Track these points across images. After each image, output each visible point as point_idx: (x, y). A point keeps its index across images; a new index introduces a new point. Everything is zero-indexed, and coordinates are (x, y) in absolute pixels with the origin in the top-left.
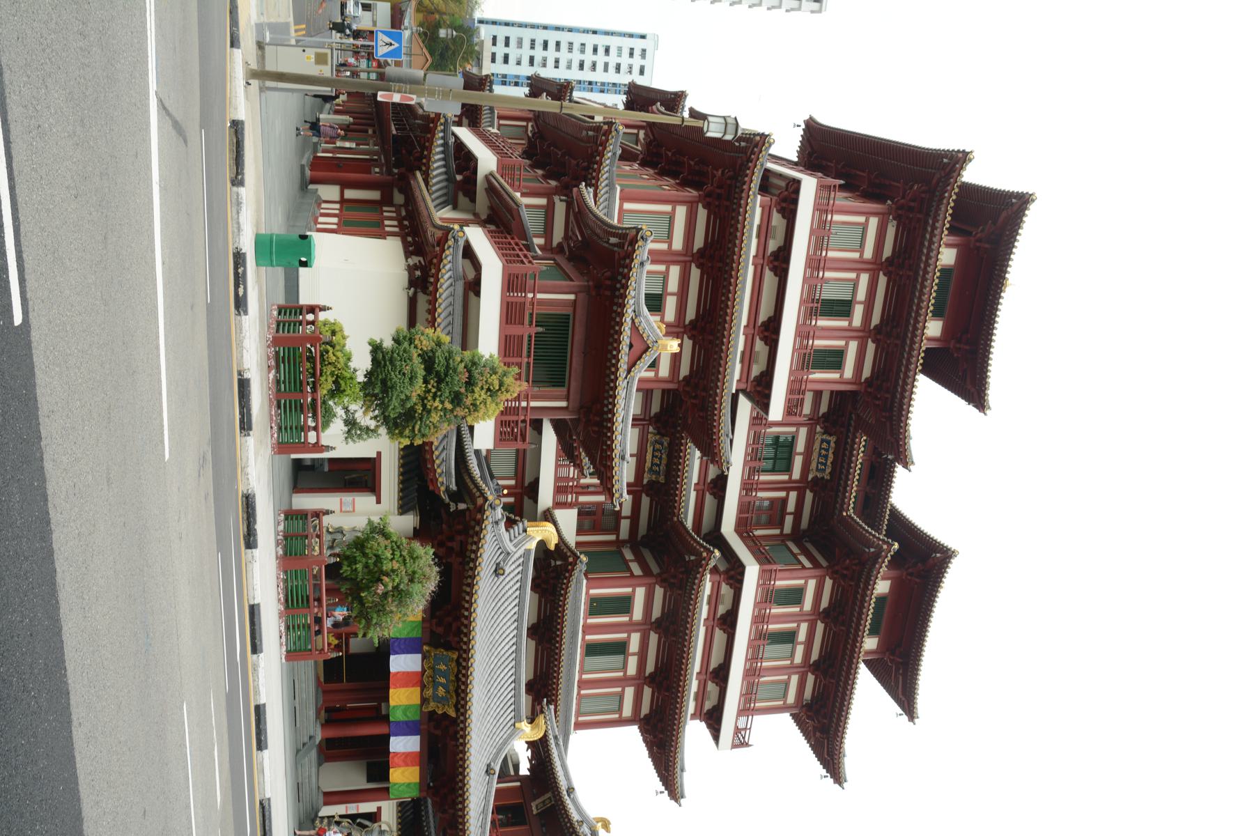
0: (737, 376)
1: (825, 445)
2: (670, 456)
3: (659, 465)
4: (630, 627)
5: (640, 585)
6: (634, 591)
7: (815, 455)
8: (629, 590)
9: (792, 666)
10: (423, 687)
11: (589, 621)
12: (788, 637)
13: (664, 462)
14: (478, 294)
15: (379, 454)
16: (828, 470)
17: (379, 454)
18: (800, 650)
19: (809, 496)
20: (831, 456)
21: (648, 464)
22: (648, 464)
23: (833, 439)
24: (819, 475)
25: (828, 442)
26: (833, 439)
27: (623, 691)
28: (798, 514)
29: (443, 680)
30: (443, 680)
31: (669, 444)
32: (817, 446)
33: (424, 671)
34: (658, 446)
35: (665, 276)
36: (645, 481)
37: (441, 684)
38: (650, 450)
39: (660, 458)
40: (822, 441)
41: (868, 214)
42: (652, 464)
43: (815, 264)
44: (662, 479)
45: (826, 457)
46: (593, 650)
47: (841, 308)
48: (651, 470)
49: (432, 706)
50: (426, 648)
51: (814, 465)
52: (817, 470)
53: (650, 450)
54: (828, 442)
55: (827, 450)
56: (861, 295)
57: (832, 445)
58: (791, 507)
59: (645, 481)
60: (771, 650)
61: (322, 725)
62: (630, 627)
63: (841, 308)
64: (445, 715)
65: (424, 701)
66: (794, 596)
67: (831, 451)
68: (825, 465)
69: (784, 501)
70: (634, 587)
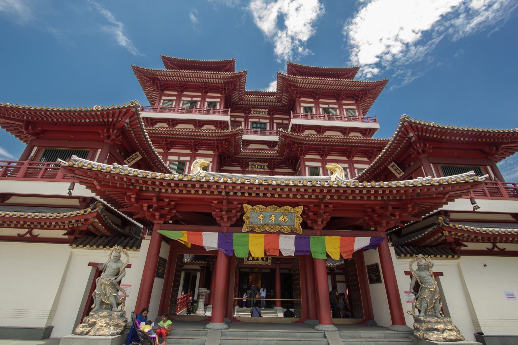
3: (261, 166)
5: (304, 164)
6: (307, 166)
7: (259, 115)
8: (307, 168)
9: (339, 108)
10: (279, 233)
12: (326, 110)
13: (259, 164)
15: (90, 264)
16: (264, 110)
17: (90, 264)
18: (331, 106)
20: (259, 110)
21: (261, 170)
22: (261, 170)
23: (252, 110)
24: (267, 113)
25: (254, 111)
26: (252, 110)
27: (356, 168)
28: (283, 119)
30: (273, 217)
31: (252, 162)
33: (265, 232)
34: (253, 167)
37: (277, 218)
40: (254, 113)
41: (160, 99)
42: (261, 168)
45: (259, 111)
47: (193, 104)
54: (254, 111)
55: (257, 111)
56: (190, 99)
57: (255, 110)
58: (280, 121)
61: (320, 323)
63: (193, 104)
66: (308, 110)
68: (262, 112)
69: (277, 124)
70: (305, 166)
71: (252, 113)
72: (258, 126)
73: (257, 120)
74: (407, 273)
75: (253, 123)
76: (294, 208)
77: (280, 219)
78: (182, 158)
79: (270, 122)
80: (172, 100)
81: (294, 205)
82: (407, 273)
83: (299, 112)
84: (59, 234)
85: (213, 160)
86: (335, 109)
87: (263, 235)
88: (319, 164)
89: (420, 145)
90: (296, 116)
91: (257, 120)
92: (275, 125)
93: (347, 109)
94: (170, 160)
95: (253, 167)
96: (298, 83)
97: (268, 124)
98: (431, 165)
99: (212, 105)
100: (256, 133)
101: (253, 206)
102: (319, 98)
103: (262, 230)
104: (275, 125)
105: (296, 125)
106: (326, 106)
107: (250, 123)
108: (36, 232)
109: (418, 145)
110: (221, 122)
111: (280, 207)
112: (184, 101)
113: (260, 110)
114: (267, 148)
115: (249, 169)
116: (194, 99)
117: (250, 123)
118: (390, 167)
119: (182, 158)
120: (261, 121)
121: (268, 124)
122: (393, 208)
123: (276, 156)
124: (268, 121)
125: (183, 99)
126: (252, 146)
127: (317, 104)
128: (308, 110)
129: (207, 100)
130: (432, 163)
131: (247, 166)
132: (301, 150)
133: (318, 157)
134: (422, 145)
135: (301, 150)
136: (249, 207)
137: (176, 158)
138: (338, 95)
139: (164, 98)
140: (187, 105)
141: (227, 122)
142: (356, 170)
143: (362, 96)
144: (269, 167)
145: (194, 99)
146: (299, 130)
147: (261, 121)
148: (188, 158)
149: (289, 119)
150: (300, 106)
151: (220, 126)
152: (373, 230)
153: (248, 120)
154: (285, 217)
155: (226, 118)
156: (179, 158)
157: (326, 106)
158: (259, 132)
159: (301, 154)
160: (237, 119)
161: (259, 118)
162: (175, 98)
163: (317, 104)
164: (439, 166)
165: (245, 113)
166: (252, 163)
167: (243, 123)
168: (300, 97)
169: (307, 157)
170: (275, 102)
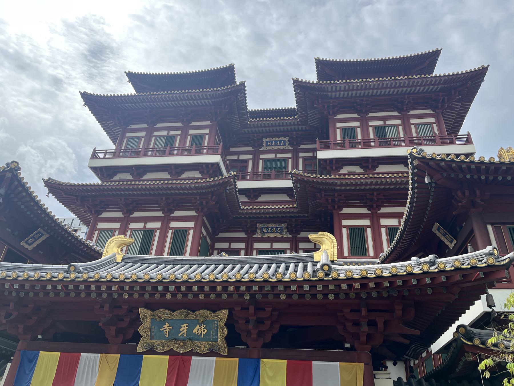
1: (269, 144)
2: (269, 222)
4: (376, 228)
5: (340, 223)
6: (345, 227)
7: (276, 148)
9: (404, 124)
11: (372, 254)
12: (380, 131)
13: (274, 225)
16: (283, 139)
18: (388, 122)
19: (302, 147)
20: (274, 139)
21: (277, 235)
22: (277, 235)
23: (264, 139)
24: (287, 143)
25: (267, 142)
26: (264, 139)
29: (184, 328)
30: (184, 328)
31: (261, 223)
34: (264, 231)
36: (291, 236)
38: (267, 235)
39: (272, 228)
40: (267, 145)
44: (284, 225)
45: (276, 142)
48: (280, 233)
49: (221, 342)
50: (140, 348)
51: (282, 147)
52: (285, 145)
53: (267, 235)
54: (267, 142)
55: (272, 142)
56: (165, 133)
59: (289, 236)
62: (376, 228)
63: (170, 140)
64: (227, 324)
65: (211, 353)
67: (273, 140)
68: (280, 141)
69: (305, 159)
71: (264, 144)
72: (274, 165)
73: (272, 156)
75: (266, 161)
76: (214, 312)
77: (195, 330)
78: (150, 225)
79: (292, 158)
80: (140, 138)
81: (214, 307)
83: (331, 138)
85: (196, 225)
86: (397, 126)
87: (167, 357)
88: (366, 222)
89: (464, 194)
90: (327, 147)
91: (272, 156)
92: (301, 161)
93: (416, 125)
94: (131, 229)
95: (264, 231)
96: (328, 91)
97: (290, 160)
98: (490, 228)
99: (198, 139)
100: (266, 177)
101: (153, 311)
102: (367, 112)
103: (166, 349)
104: (301, 161)
105: (325, 160)
106: (381, 123)
107: (261, 162)
109: (459, 193)
110: (207, 164)
111: (194, 311)
112: (157, 137)
113: (277, 139)
114: (287, 199)
115: (258, 235)
116: (172, 133)
117: (261, 162)
118: (435, 229)
119: (150, 225)
120: (279, 156)
121: (290, 160)
122: (369, 311)
123: (298, 212)
124: (289, 155)
125: (156, 133)
126: (263, 198)
127: (364, 122)
128: (349, 133)
129: (191, 132)
130: (492, 224)
131: (255, 232)
132: (333, 201)
133: (364, 210)
134: (467, 193)
135: (333, 201)
136: (148, 312)
137: (140, 225)
138: (402, 104)
139: (128, 135)
140: (161, 144)
141: (217, 164)
143: (444, 100)
144: (289, 231)
145: (172, 133)
146: (332, 168)
147: (279, 156)
148: (158, 225)
149: (314, 150)
150: (335, 128)
151: (208, 172)
152: (347, 349)
153: (259, 156)
154: (203, 327)
155: (216, 158)
156: (145, 225)
158: (273, 175)
159: (334, 207)
160: (242, 157)
162: (143, 134)
163: (364, 122)
164: (504, 229)
165: (253, 146)
166: (261, 225)
167: (250, 163)
168: (335, 114)
169: (345, 211)
170: (298, 125)
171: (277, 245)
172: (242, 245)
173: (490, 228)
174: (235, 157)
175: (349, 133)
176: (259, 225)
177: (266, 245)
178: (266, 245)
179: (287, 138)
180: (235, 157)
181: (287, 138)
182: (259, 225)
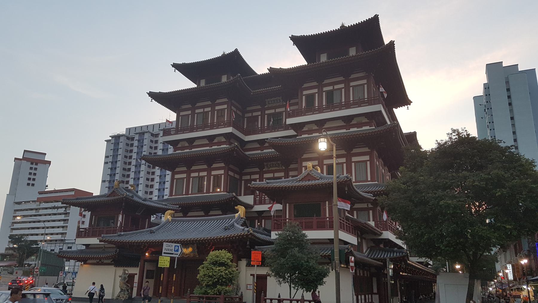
0: (225, 146)
7: (274, 105)
12: (330, 94)
14: (90, 245)
18: (336, 87)
20: (273, 99)
23: (266, 100)
26: (266, 100)
32: (270, 105)
35: (194, 177)
38: (271, 169)
43: (192, 130)
46: (200, 190)
51: (278, 104)
53: (271, 169)
54: (268, 101)
60: (336, 100)
73: (272, 111)
74: (251, 275)
82: (251, 275)
84: (109, 261)
106: (331, 88)
108: (102, 261)
137: (196, 174)
142: (353, 164)
155: (229, 130)
157: (331, 88)
161: (275, 108)
171: (277, 175)
172: (257, 176)
173: (287, 205)
174: (250, 115)
175: (310, 98)
176: (265, 164)
177: (271, 175)
178: (271, 175)
179: (280, 98)
180: (250, 115)
181: (280, 98)
182: (265, 164)
